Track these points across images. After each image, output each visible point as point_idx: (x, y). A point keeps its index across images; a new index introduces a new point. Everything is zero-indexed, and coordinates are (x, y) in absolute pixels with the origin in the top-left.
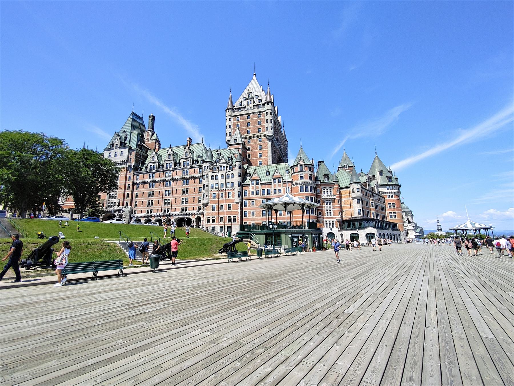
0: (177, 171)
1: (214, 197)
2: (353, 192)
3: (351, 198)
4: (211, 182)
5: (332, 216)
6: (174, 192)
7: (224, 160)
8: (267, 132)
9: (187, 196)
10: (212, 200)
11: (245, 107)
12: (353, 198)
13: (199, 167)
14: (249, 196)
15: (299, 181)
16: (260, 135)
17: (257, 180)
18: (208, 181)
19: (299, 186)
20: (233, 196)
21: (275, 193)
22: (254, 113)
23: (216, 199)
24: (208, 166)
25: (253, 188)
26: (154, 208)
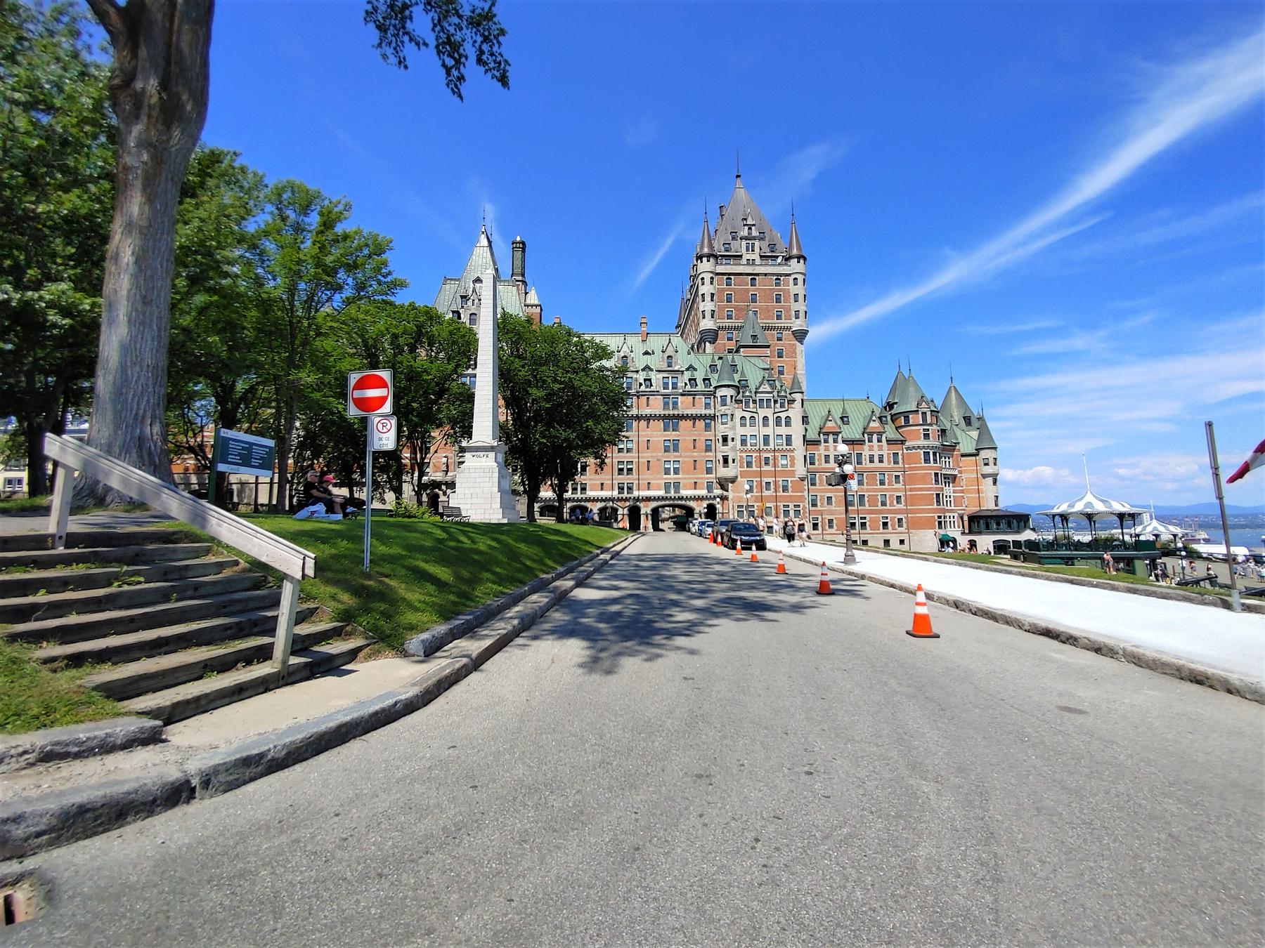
0: (648, 398)
1: (749, 464)
2: (986, 464)
3: (979, 475)
4: (741, 431)
5: (953, 508)
6: (643, 445)
7: (767, 386)
8: (798, 322)
9: (678, 457)
10: (745, 469)
11: (741, 256)
12: (984, 476)
13: (704, 395)
14: (820, 464)
15: (922, 442)
16: (780, 325)
17: (836, 434)
18: (733, 428)
19: (922, 452)
20: (793, 465)
21: (872, 461)
22: (766, 275)
23: (754, 468)
24: (732, 396)
25: (827, 449)
26: (591, 479)
